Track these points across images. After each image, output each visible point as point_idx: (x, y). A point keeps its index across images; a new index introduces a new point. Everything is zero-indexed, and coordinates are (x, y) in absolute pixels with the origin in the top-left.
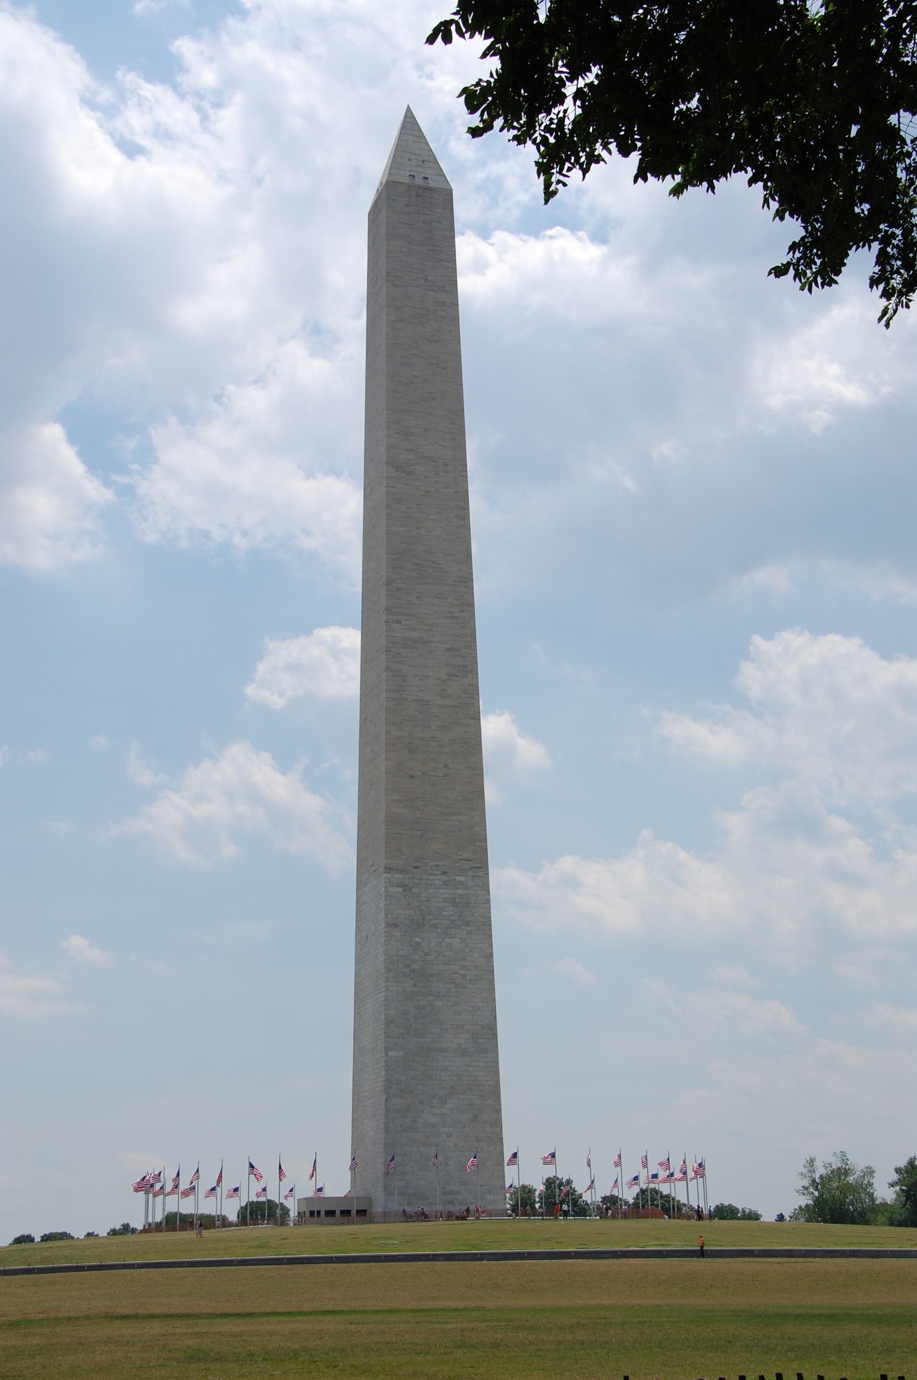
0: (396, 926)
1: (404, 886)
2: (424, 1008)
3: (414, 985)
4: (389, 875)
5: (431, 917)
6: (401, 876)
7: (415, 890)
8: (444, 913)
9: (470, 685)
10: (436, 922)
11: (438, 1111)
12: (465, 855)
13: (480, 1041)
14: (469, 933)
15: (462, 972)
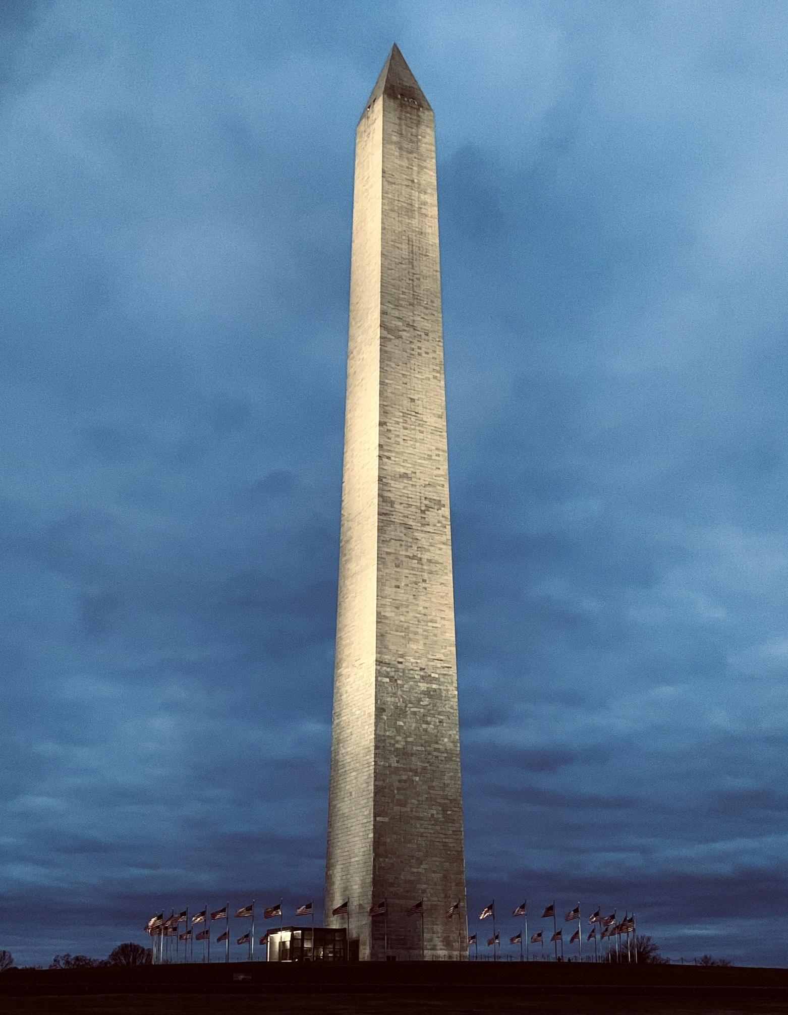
2: (405, 781)
3: (398, 762)
4: (379, 668)
6: (389, 670)
7: (399, 682)
9: (443, 516)
10: (415, 709)
11: (416, 870)
12: (438, 656)
13: (449, 812)
15: (435, 754)
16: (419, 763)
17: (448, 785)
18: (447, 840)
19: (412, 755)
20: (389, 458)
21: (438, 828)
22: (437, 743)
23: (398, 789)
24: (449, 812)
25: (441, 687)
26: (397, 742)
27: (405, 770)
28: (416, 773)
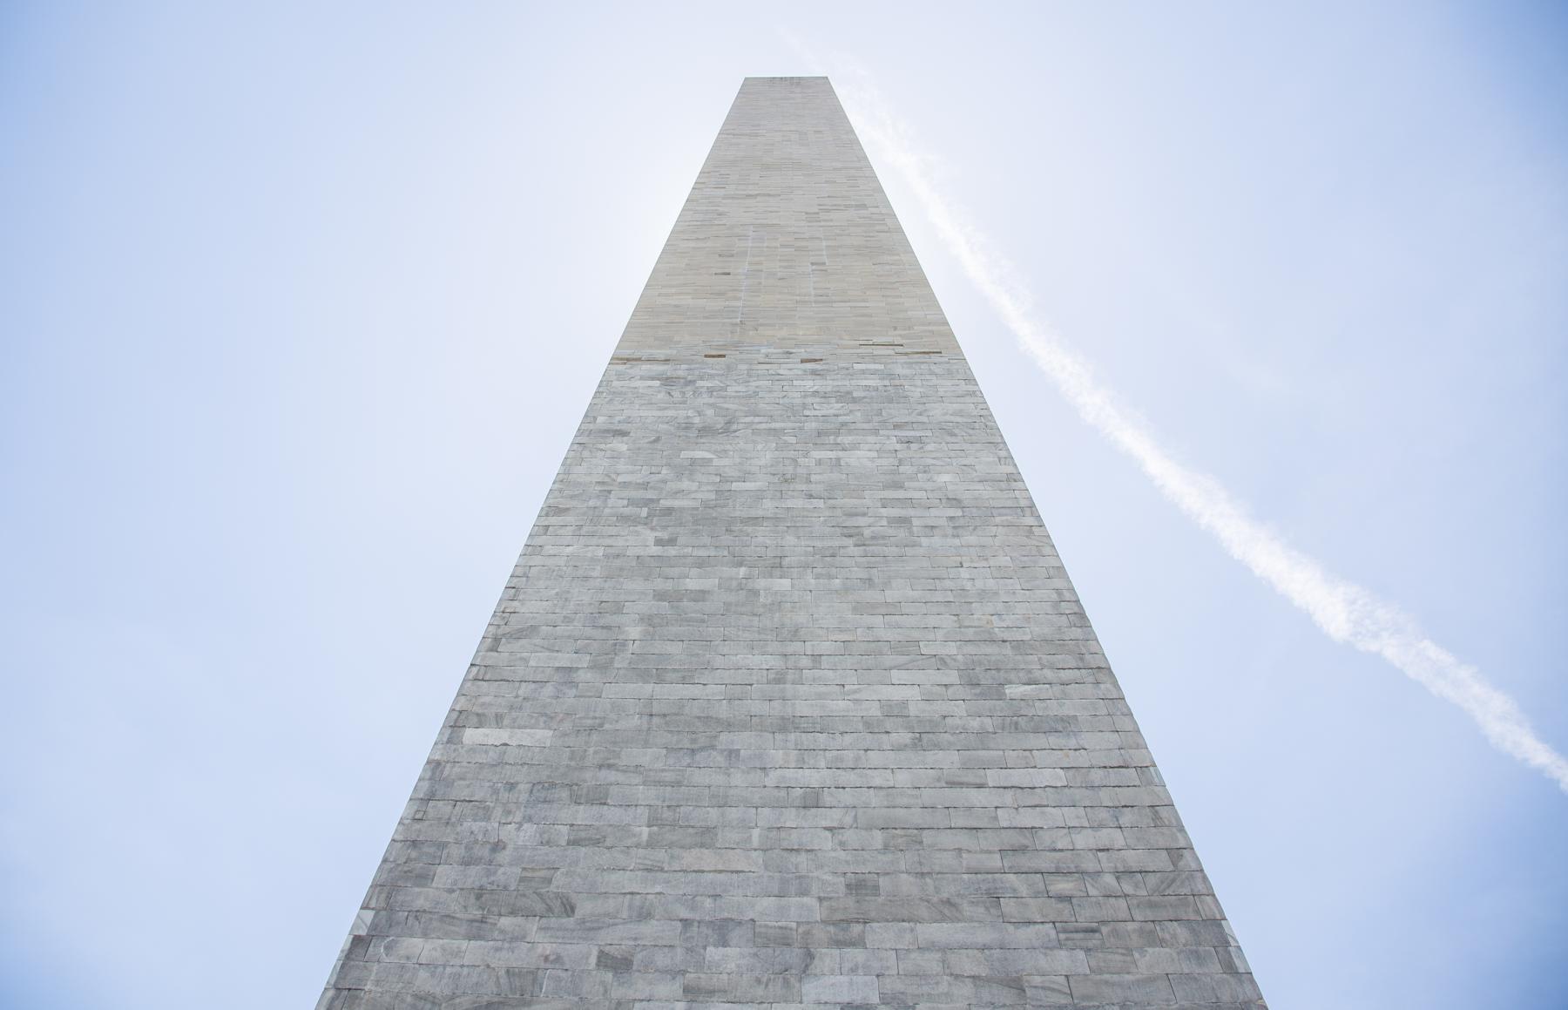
1: (667, 381)
2: (701, 595)
5: (757, 419)
6: (659, 368)
8: (807, 413)
13: (1014, 691)
16: (790, 540)
17: (983, 595)
18: (1028, 818)
19: (755, 521)
23: (647, 619)
25: (897, 382)
26: (677, 493)
27: (701, 563)
28: (777, 566)
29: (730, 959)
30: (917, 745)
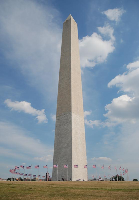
0: (57, 127)
3: (59, 137)
12: (68, 110)
14: (68, 124)
20: (61, 77)
21: (66, 149)
22: (67, 130)
24: (69, 145)
29: (61, 158)
30: (66, 148)
